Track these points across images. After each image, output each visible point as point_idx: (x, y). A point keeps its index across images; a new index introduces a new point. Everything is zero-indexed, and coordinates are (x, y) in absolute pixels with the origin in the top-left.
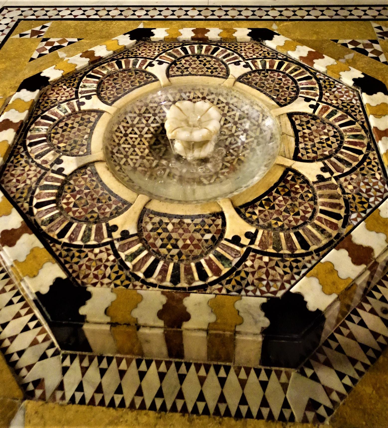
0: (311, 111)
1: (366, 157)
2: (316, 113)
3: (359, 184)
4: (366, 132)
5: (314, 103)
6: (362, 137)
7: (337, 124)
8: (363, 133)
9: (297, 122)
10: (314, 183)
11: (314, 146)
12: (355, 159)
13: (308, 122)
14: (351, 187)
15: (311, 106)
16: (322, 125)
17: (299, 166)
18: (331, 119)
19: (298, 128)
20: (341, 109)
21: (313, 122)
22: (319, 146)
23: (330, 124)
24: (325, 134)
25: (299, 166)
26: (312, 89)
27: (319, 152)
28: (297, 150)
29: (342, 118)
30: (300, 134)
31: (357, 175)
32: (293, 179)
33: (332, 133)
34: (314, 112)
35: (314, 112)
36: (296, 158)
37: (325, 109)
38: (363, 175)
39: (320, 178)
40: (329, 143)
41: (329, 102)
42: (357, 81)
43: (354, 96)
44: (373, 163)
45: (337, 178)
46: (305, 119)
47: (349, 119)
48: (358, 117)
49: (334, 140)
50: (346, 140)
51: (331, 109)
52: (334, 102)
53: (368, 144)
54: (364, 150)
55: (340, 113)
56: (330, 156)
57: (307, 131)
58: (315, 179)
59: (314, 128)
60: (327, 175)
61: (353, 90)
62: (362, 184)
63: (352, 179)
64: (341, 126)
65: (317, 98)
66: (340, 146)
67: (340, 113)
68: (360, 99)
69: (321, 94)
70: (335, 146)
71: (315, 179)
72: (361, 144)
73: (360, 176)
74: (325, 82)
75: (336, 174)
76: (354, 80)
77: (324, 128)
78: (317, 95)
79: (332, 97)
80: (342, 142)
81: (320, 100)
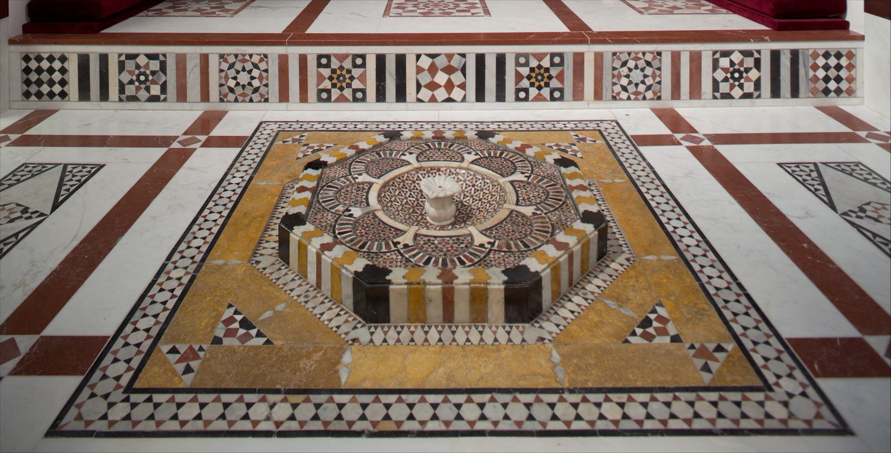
0: (526, 179)
1: (564, 203)
2: (530, 180)
3: (560, 216)
4: (564, 189)
5: (528, 175)
6: (561, 192)
7: (544, 186)
8: (562, 190)
9: (516, 186)
10: (530, 216)
11: (530, 198)
12: (557, 204)
13: (524, 186)
14: (555, 218)
15: (525, 176)
16: (534, 187)
17: (519, 208)
18: (540, 183)
19: (517, 189)
20: (547, 178)
21: (528, 186)
22: (533, 198)
23: (539, 186)
24: (537, 192)
25: (519, 208)
26: (526, 167)
27: (533, 201)
28: (518, 201)
29: (547, 182)
30: (519, 192)
31: (559, 211)
32: (516, 215)
33: (541, 191)
34: (528, 180)
35: (528, 180)
36: (517, 204)
37: (534, 179)
38: (563, 211)
39: (534, 214)
40: (540, 196)
41: (538, 174)
42: (556, 161)
43: (555, 170)
44: (569, 205)
45: (545, 214)
46: (522, 184)
47: (553, 183)
48: (559, 182)
49: (543, 194)
50: (551, 194)
51: (540, 178)
52: (542, 174)
53: (566, 196)
54: (563, 199)
55: (546, 180)
56: (541, 203)
57: (524, 191)
58: (531, 215)
59: (528, 189)
60: (539, 212)
61: (555, 167)
62: (562, 216)
63: (555, 214)
64: (547, 187)
65: (530, 172)
66: (547, 198)
67: (546, 180)
68: (560, 172)
69: (532, 170)
70: (544, 197)
71: (531, 215)
72: (560, 196)
73: (561, 212)
74: (534, 163)
75: (545, 211)
76: (554, 160)
77: (536, 189)
78: (529, 170)
79: (540, 171)
80: (548, 196)
81: (532, 173)
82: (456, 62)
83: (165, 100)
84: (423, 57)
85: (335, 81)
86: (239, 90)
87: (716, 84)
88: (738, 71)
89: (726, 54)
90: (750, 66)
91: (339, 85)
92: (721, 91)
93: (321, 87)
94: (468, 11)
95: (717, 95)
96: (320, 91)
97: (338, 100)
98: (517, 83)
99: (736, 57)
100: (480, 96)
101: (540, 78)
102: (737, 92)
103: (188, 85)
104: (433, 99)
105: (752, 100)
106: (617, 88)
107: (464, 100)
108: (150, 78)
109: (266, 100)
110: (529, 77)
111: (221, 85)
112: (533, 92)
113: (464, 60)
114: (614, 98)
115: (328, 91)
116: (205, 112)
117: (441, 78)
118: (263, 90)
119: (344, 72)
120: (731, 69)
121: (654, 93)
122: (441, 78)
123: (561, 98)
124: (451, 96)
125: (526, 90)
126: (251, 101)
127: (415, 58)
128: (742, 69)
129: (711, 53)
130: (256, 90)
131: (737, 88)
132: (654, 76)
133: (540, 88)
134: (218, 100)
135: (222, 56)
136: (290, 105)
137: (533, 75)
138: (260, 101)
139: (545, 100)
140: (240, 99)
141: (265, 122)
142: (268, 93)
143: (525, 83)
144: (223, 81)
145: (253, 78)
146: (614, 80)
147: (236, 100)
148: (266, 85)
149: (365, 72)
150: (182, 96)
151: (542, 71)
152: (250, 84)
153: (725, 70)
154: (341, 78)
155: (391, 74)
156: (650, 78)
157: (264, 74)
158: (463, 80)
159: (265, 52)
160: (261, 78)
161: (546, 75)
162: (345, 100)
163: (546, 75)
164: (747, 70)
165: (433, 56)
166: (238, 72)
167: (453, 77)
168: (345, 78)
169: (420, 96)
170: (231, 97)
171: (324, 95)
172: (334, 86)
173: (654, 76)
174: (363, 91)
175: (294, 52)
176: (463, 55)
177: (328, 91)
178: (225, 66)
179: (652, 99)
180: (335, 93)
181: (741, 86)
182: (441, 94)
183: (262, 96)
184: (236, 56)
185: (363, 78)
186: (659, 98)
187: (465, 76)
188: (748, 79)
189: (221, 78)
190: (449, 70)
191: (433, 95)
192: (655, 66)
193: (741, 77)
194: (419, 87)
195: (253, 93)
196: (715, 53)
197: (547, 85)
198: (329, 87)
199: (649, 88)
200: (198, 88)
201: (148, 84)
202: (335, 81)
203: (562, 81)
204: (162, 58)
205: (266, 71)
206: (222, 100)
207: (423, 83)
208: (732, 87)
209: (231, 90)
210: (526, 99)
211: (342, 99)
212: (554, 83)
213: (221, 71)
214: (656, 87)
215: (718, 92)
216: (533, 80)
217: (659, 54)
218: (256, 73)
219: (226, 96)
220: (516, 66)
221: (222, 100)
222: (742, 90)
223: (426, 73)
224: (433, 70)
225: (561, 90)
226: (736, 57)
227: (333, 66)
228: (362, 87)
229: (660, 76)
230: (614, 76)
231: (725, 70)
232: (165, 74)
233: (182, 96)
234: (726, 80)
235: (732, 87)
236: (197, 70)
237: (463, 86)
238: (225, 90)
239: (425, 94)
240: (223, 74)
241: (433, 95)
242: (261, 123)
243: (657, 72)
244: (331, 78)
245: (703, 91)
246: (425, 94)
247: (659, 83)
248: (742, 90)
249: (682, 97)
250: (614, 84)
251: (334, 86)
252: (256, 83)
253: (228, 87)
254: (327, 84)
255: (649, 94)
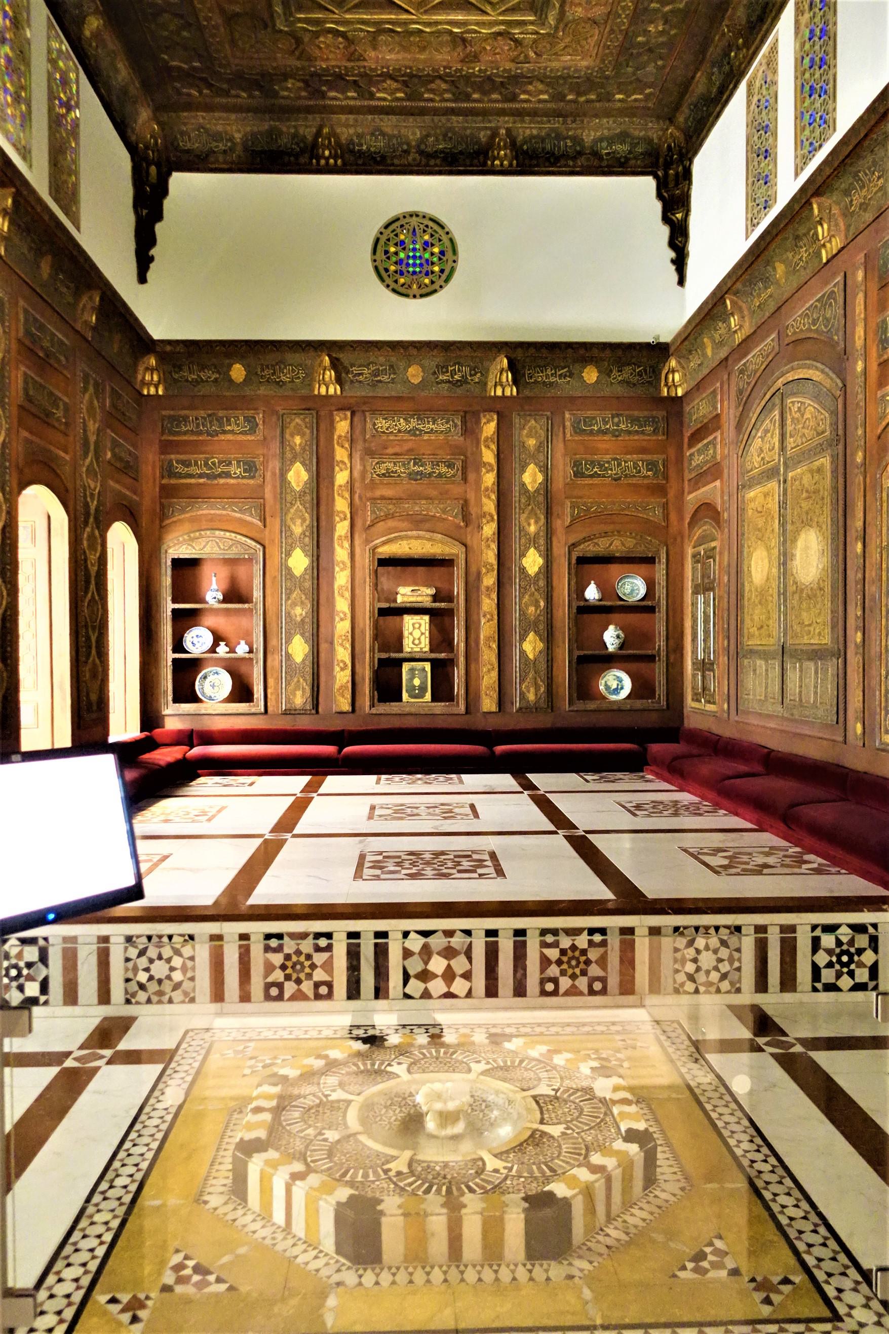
82: (458, 941)
83: (46, 1003)
84: (412, 935)
85: (289, 971)
86: (153, 987)
87: (816, 972)
88: (847, 952)
89: (830, 929)
90: (863, 946)
91: (294, 976)
92: (824, 980)
93: (270, 979)
94: (475, 872)
95: (819, 986)
96: (268, 986)
97: (293, 998)
98: (542, 971)
99: (845, 933)
100: (492, 991)
101: (574, 963)
102: (845, 982)
103: (80, 981)
104: (426, 995)
105: (867, 993)
106: (681, 977)
107: (469, 994)
108: (25, 972)
109: (192, 1000)
110: (559, 962)
111: (128, 980)
112: (565, 983)
113: (468, 940)
114: (677, 991)
115: (280, 986)
116: (105, 1019)
117: (437, 965)
118: (187, 985)
119: (302, 958)
120: (838, 951)
121: (732, 984)
122: (437, 965)
123: (604, 992)
124: (452, 990)
125: (555, 981)
126: (170, 1001)
127: (400, 936)
128: (852, 950)
129: (809, 928)
130: (177, 986)
131: (845, 977)
132: (731, 960)
133: (573, 977)
134: (123, 1000)
135: (129, 939)
136: (226, 1006)
137: (565, 959)
138: (183, 1002)
139: (581, 994)
140: (155, 999)
141: (192, 1030)
142: (194, 990)
143: (554, 970)
144: (130, 975)
145: (172, 969)
146: (676, 966)
147: (149, 1001)
148: (192, 979)
149: (332, 957)
150: (71, 997)
151: (577, 954)
152: (169, 977)
153: (830, 952)
154: (298, 967)
155: (367, 959)
156: (726, 963)
157: (189, 964)
158: (468, 967)
159: (190, 932)
160: (184, 969)
161: (583, 959)
162: (305, 998)
163: (583, 959)
164: (860, 952)
165: (426, 934)
166: (151, 961)
167: (453, 963)
168: (303, 967)
169: (408, 990)
170: (142, 996)
171: (274, 992)
172: (288, 978)
173: (731, 960)
174: (330, 985)
175: (232, 929)
176: (468, 933)
177: (280, 986)
178: (133, 953)
179: (728, 992)
180: (290, 988)
181: (851, 974)
182: (437, 986)
183: (186, 994)
184: (149, 938)
185: (328, 966)
186: (738, 991)
187: (471, 962)
188: (861, 965)
189: (127, 970)
190: (449, 953)
191: (426, 989)
192: (732, 947)
193: (851, 961)
194: (406, 978)
195: (173, 990)
196: (814, 928)
197: (584, 973)
198: (282, 979)
199: (724, 976)
200: (94, 984)
201: (22, 980)
202: (289, 971)
203: (604, 967)
204: (41, 942)
205: (192, 958)
206: (128, 1002)
207: (412, 972)
208: (839, 975)
209: (142, 987)
210: (555, 993)
211: (299, 996)
212: (595, 970)
213: (127, 960)
214: (734, 976)
215: (819, 981)
216: (565, 966)
217: (738, 929)
218: (177, 962)
219: (134, 995)
220: (541, 947)
221: (128, 1002)
222: (853, 978)
223: (416, 957)
224: (426, 952)
225: (603, 980)
226: (845, 933)
227: (287, 950)
228: (327, 978)
229: (739, 960)
230: (675, 961)
231: (830, 952)
232: (47, 966)
233: (71, 997)
234: (830, 965)
235: (839, 975)
236: (94, 960)
237: (467, 976)
238: (133, 987)
239: (416, 986)
240: (130, 965)
241: (426, 989)
242: (186, 1032)
243: (736, 955)
244: (283, 967)
245: (799, 980)
246: (416, 986)
247: (739, 969)
248: (853, 978)
249: (770, 989)
250: (677, 971)
251: (288, 978)
252: (177, 976)
253: (138, 983)
254: (278, 976)
255: (725, 985)
